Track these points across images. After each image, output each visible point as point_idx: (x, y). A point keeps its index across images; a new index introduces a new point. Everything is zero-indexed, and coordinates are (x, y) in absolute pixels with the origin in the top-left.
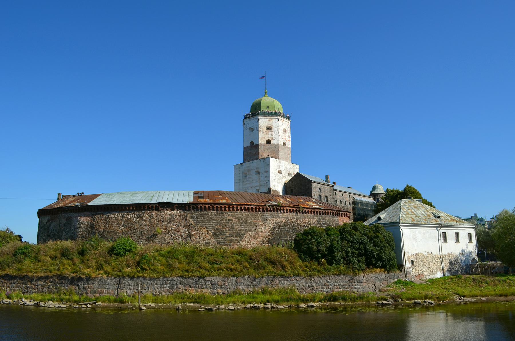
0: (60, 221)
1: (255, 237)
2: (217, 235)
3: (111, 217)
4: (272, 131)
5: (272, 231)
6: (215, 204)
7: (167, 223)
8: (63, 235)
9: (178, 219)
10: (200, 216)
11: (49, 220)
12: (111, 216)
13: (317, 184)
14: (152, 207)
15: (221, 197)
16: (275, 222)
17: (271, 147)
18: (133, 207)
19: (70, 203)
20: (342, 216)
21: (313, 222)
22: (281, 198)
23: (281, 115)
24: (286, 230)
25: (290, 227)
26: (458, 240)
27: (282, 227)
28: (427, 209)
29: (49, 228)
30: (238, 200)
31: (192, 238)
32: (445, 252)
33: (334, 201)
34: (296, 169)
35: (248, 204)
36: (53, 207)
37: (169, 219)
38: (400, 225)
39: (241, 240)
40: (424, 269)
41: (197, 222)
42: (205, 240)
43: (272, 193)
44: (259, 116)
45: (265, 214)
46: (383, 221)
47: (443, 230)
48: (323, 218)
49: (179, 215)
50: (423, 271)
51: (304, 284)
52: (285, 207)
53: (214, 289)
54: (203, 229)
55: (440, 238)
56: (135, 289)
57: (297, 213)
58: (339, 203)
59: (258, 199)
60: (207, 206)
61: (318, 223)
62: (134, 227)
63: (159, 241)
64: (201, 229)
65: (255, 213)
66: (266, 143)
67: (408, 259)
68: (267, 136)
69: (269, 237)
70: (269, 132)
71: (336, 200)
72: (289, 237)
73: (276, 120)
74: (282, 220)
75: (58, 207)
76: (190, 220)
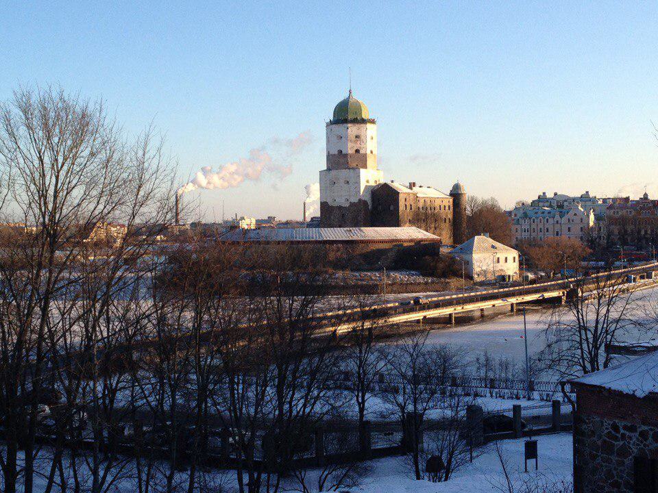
4: (360, 140)
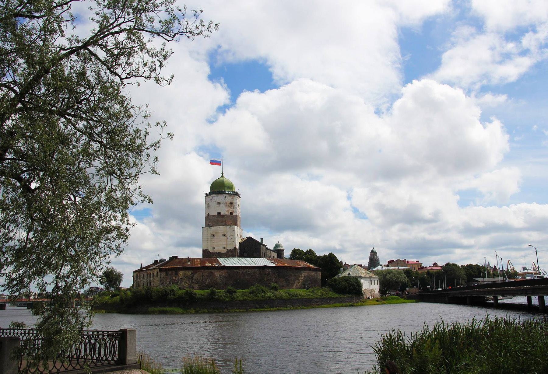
0: (202, 274)
4: (233, 206)
11: (192, 273)
26: (374, 284)
29: (192, 278)
70: (231, 206)
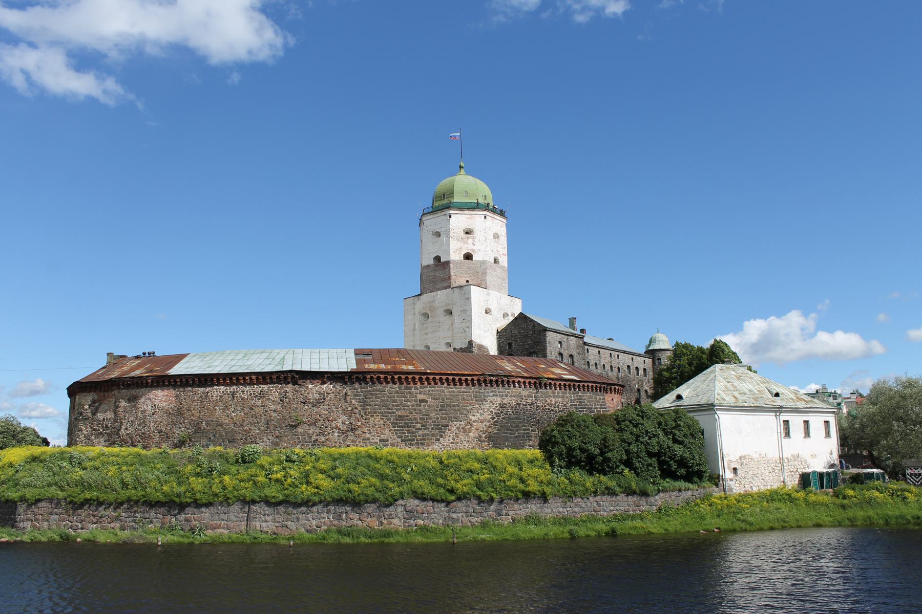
1: (465, 431)
2: (400, 427)
3: (212, 396)
4: (473, 238)
5: (495, 420)
6: (396, 373)
7: (313, 406)
8: (123, 427)
9: (332, 399)
10: (371, 394)
11: (94, 402)
12: (211, 394)
13: (555, 333)
14: (286, 378)
15: (404, 359)
16: (500, 404)
17: (472, 266)
18: (251, 379)
19: (133, 371)
20: (611, 393)
21: (562, 403)
22: (506, 360)
23: (486, 208)
24: (518, 418)
25: (524, 413)
26: (807, 434)
27: (511, 413)
28: (758, 382)
30: (434, 366)
31: (357, 433)
32: (787, 454)
33: (585, 365)
34: (516, 307)
35: (453, 372)
36: (101, 379)
37: (315, 399)
38: (716, 409)
39: (441, 436)
40: (754, 482)
41: (364, 404)
42: (380, 436)
43: (475, 350)
44: (450, 210)
45: (483, 391)
46: (686, 401)
47: (784, 417)
48: (580, 396)
49: (333, 393)
50: (752, 485)
51: (561, 510)
52: (516, 377)
53: (410, 519)
54: (376, 416)
55: (779, 431)
56: (274, 520)
57: (536, 388)
58: (593, 368)
59: (468, 364)
60: (382, 376)
61: (572, 405)
62: (254, 413)
63: (299, 438)
64: (373, 416)
65: (464, 389)
66: (463, 259)
67: (729, 465)
68: (465, 246)
69: (490, 430)
70: (468, 238)
71: (588, 362)
72: (524, 430)
73: (481, 217)
74: (511, 400)
75: (111, 379)
76: (353, 401)
